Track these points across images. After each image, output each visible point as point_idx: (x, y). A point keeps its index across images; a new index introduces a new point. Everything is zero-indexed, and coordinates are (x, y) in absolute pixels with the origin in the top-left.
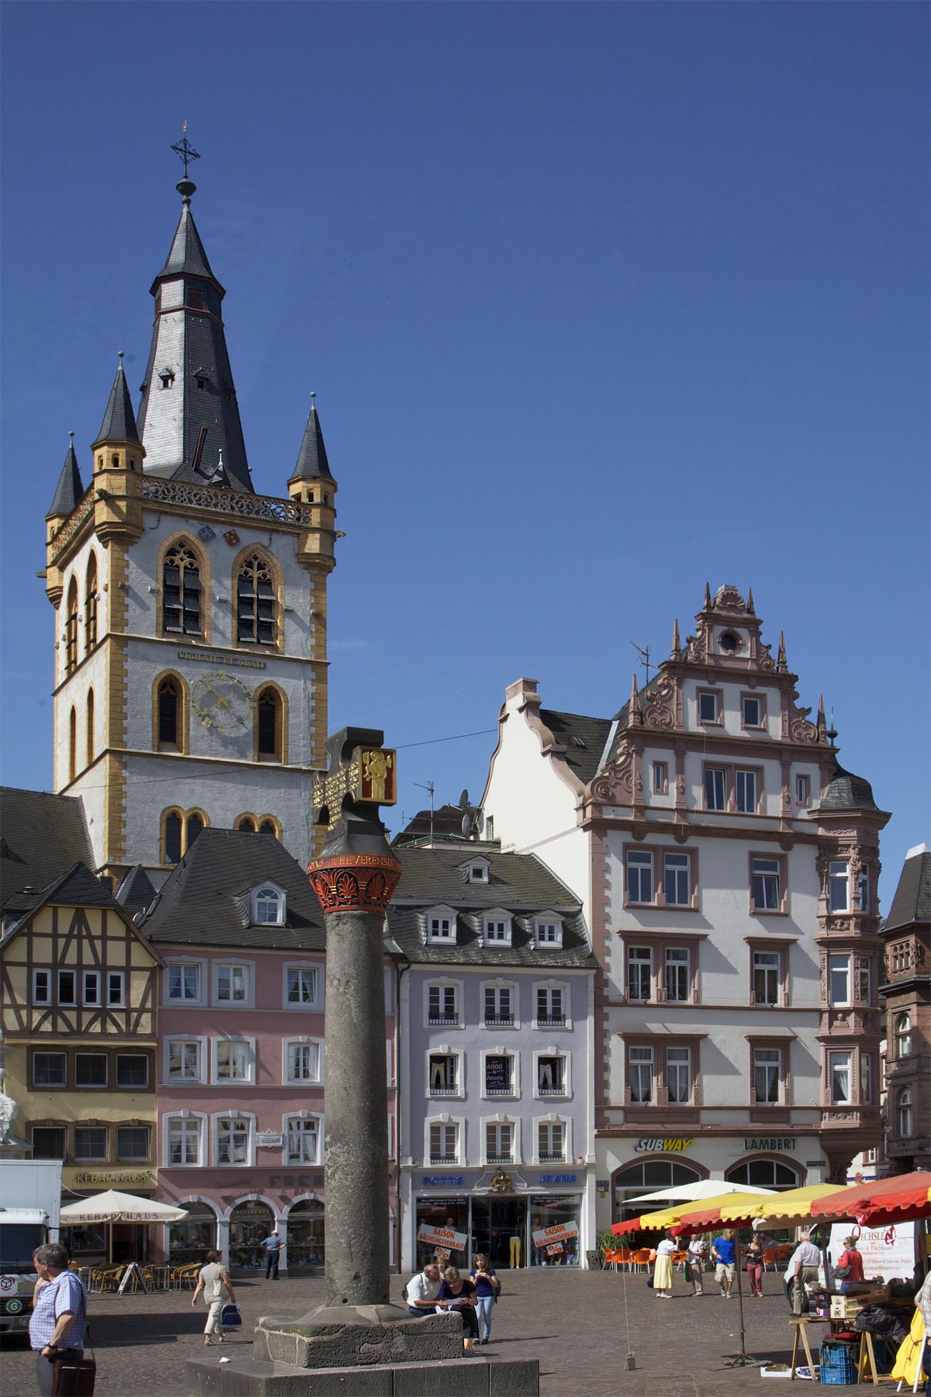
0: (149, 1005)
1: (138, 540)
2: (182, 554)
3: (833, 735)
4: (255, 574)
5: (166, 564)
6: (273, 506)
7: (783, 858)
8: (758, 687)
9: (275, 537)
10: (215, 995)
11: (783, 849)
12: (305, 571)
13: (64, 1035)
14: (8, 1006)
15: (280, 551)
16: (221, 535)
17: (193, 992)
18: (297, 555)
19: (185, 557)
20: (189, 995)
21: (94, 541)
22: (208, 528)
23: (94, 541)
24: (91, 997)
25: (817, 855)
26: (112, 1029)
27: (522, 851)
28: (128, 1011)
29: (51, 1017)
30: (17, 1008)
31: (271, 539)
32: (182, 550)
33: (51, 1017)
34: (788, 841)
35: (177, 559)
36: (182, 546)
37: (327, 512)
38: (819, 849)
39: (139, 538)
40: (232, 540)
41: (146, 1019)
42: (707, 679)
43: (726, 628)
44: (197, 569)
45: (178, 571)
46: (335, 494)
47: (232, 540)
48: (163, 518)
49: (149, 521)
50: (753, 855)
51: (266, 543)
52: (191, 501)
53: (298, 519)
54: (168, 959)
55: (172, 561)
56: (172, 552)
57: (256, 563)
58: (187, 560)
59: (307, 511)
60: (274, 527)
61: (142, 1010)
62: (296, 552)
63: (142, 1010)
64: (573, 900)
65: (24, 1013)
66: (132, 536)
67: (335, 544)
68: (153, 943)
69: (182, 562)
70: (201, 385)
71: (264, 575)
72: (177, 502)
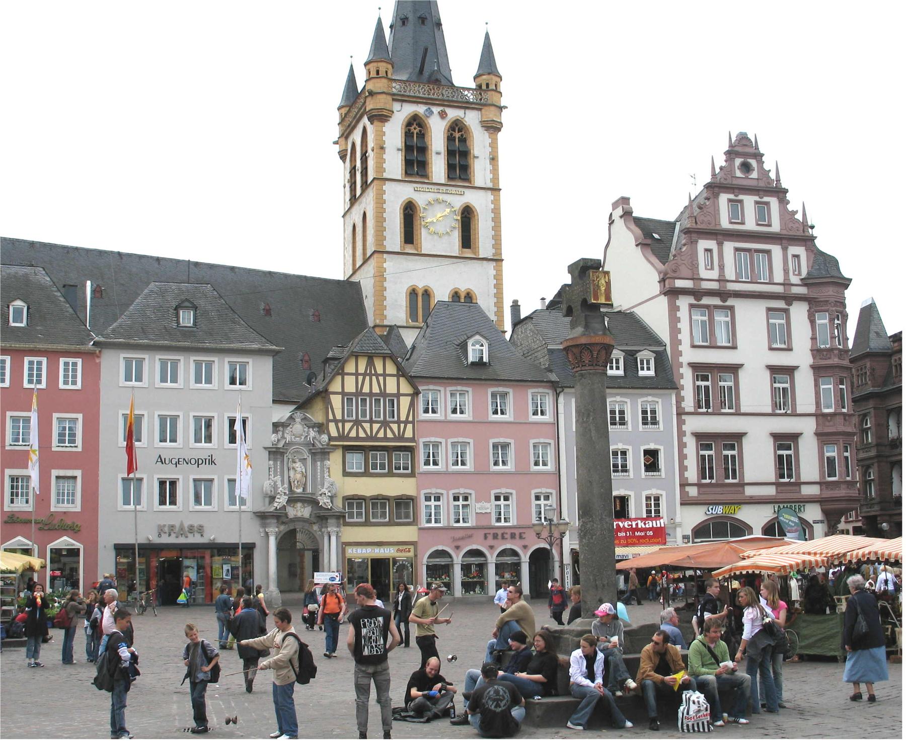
0: (411, 419)
3: (812, 227)
4: (457, 135)
5: (406, 133)
6: (466, 93)
7: (786, 311)
8: (765, 198)
9: (467, 111)
10: (449, 411)
11: (786, 305)
13: (363, 439)
14: (331, 421)
15: (472, 119)
16: (437, 112)
17: (436, 409)
19: (417, 127)
20: (434, 412)
21: (365, 119)
22: (429, 108)
23: (365, 119)
24: (378, 414)
25: (808, 308)
26: (390, 435)
27: (626, 310)
28: (399, 422)
30: (336, 421)
34: (790, 299)
35: (412, 128)
36: (415, 120)
37: (497, 94)
38: (809, 304)
39: (391, 117)
40: (443, 115)
41: (410, 426)
42: (733, 193)
43: (743, 160)
44: (423, 135)
45: (413, 137)
46: (501, 83)
47: (443, 115)
49: (396, 106)
50: (769, 309)
52: (419, 92)
53: (481, 100)
54: (421, 388)
55: (409, 130)
56: (409, 124)
58: (418, 129)
60: (466, 105)
61: (406, 422)
63: (406, 422)
64: (660, 343)
65: (340, 425)
66: (387, 116)
67: (502, 113)
68: (412, 380)
69: (415, 130)
70: (423, 23)
71: (462, 135)
72: (412, 94)
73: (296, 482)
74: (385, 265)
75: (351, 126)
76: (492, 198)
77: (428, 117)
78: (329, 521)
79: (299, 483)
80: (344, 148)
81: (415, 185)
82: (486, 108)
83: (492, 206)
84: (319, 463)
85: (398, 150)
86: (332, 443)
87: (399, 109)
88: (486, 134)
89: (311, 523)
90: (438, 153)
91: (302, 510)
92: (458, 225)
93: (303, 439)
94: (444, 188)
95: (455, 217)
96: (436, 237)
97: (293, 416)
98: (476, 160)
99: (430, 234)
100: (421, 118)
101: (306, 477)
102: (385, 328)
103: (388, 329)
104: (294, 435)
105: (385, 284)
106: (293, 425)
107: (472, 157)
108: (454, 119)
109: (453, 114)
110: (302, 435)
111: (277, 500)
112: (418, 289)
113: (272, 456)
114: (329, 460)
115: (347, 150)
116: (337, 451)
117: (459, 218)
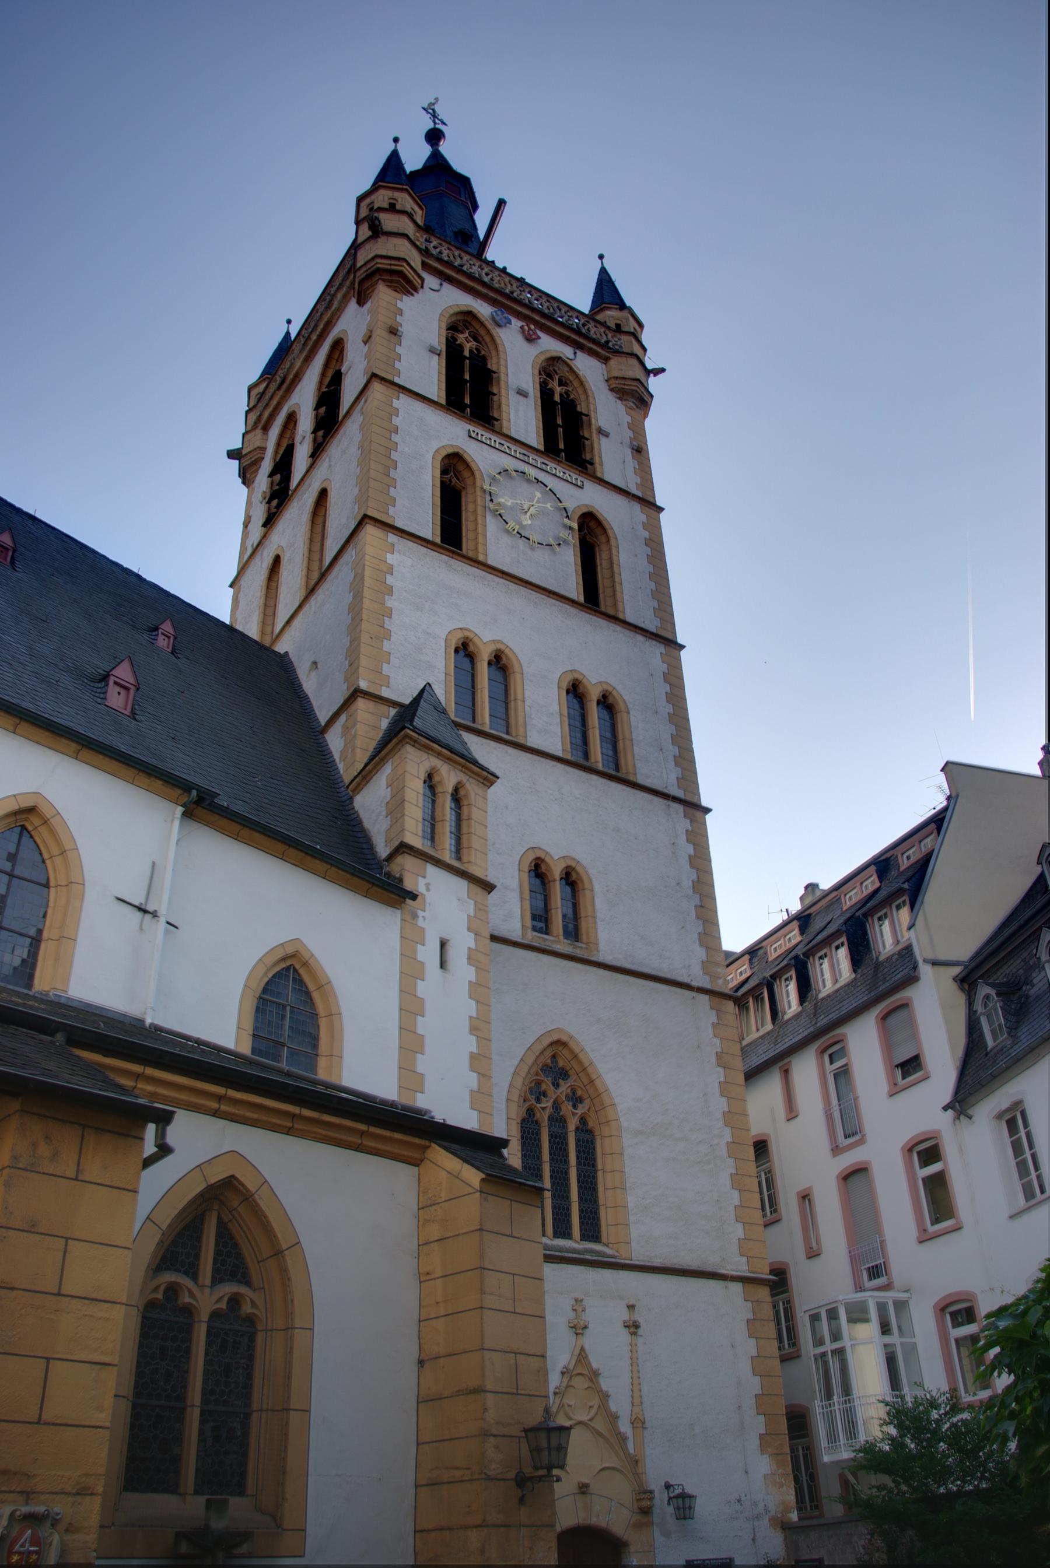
1: (415, 294)
2: (467, 335)
9: (579, 354)
12: (619, 402)
18: (607, 381)
31: (575, 353)
32: (467, 332)
39: (418, 293)
47: (530, 339)
48: (446, 285)
51: (571, 356)
57: (557, 377)
59: (616, 339)
62: (606, 378)
66: (409, 282)
71: (567, 393)
74: (390, 558)
75: (288, 382)
76: (644, 518)
77: (499, 326)
80: (258, 444)
81: (472, 428)
82: (622, 360)
83: (646, 534)
85: (432, 350)
87: (436, 287)
88: (620, 407)
90: (522, 393)
92: (574, 539)
94: (540, 460)
95: (566, 521)
96: (521, 543)
98: (604, 440)
99: (507, 531)
100: (482, 324)
102: (384, 708)
103: (393, 711)
105: (390, 602)
107: (594, 428)
108: (554, 354)
109: (550, 345)
112: (476, 640)
115: (263, 449)
117: (575, 526)
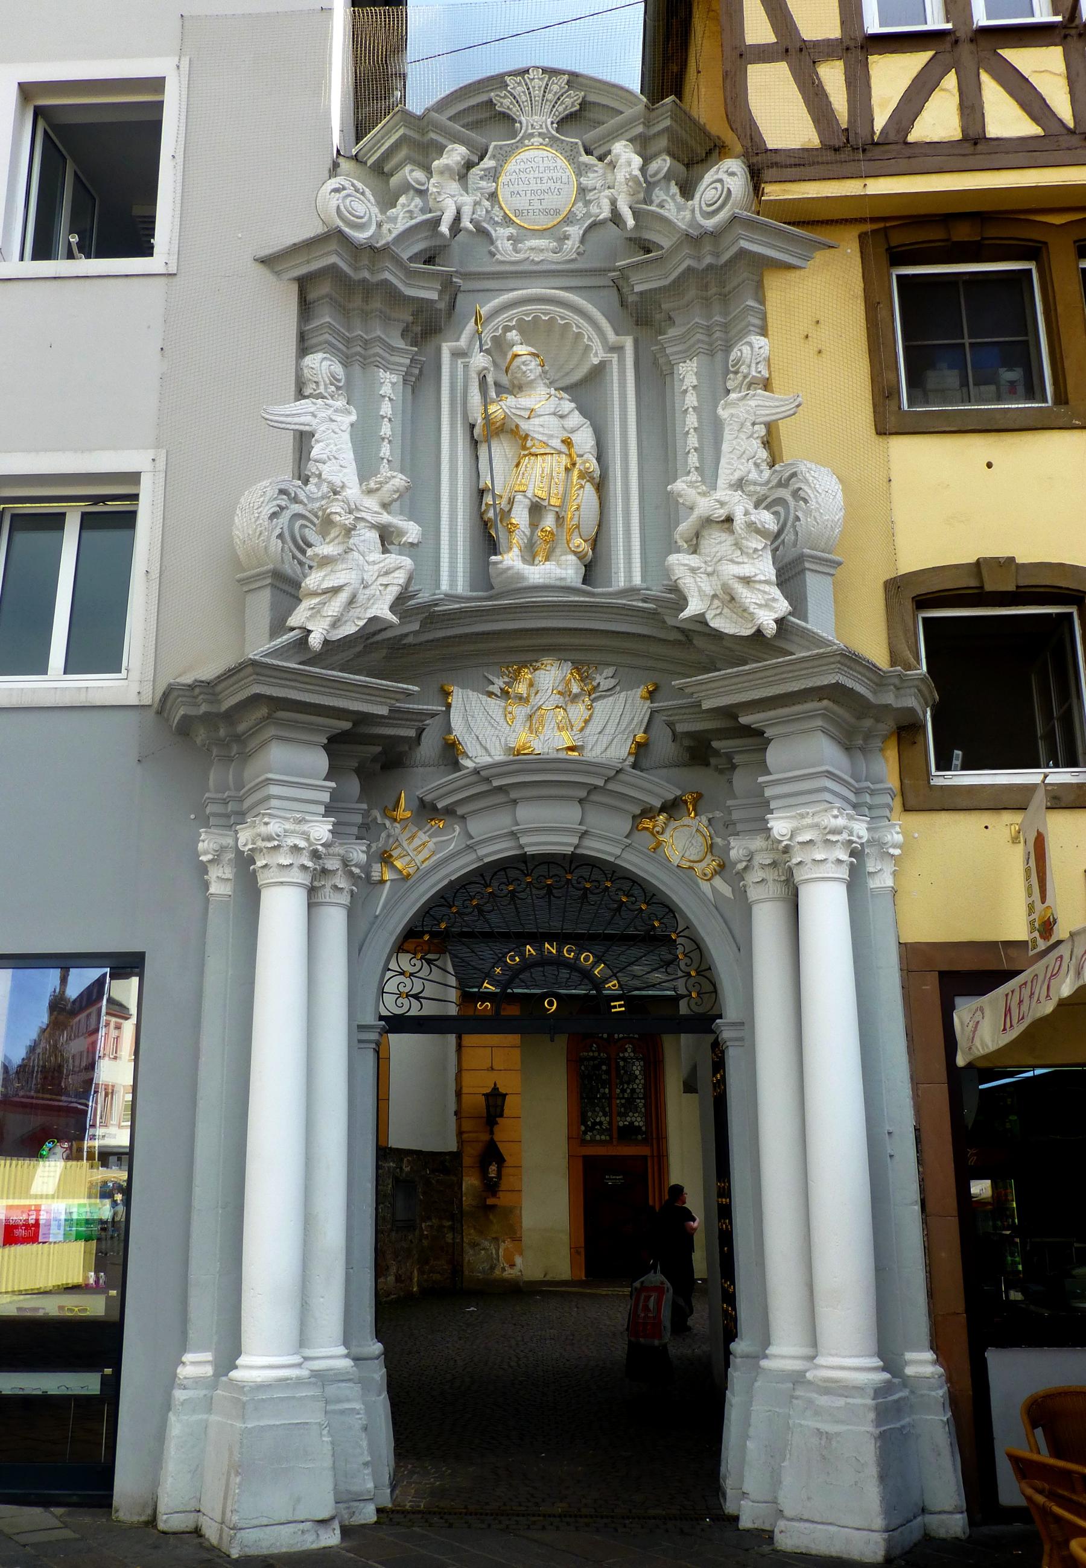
14: (764, 54)
29: (951, 81)
33: (951, 81)
73: (520, 516)
78: (774, 755)
79: (549, 522)
84: (688, 373)
86: (774, 192)
89: (648, 812)
91: (578, 711)
93: (572, 244)
97: (504, 103)
101: (601, 486)
104: (507, 221)
106: (503, 157)
110: (569, 219)
111: (314, 580)
113: (325, 317)
114: (764, 332)
116: (820, 256)
